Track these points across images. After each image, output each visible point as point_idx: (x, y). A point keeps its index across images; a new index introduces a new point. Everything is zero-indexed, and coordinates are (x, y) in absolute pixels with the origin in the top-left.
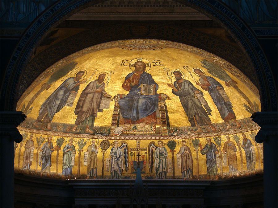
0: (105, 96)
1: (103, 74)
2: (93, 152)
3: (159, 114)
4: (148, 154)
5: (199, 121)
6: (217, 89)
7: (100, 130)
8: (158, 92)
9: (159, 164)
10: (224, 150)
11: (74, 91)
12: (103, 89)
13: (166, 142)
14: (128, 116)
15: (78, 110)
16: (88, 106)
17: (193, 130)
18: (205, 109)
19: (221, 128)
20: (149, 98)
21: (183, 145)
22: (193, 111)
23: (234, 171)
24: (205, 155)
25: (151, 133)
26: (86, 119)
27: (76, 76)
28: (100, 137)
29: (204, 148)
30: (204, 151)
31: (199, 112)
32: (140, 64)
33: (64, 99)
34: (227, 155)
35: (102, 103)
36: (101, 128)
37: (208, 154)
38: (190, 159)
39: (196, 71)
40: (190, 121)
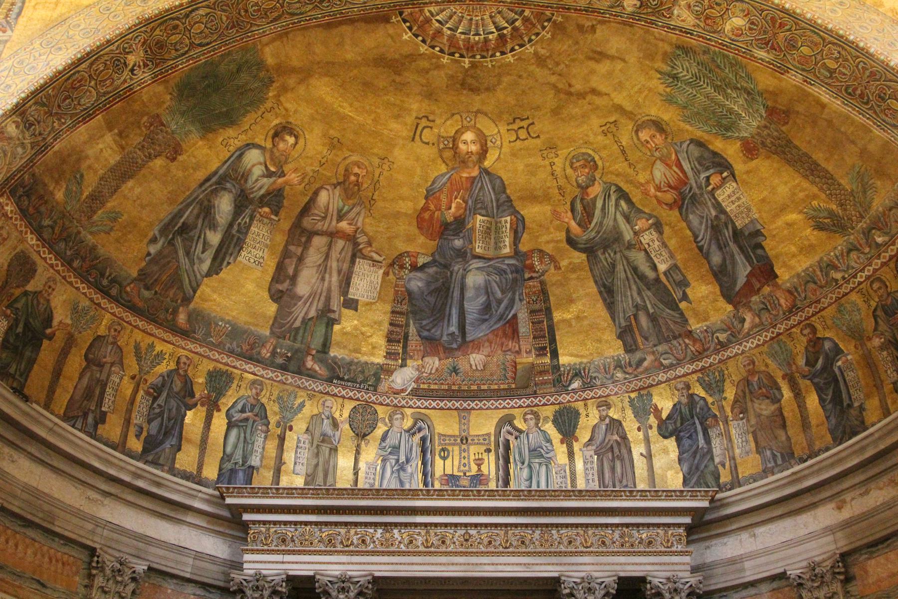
0: (364, 251)
1: (358, 164)
2: (325, 438)
3: (524, 327)
4: (493, 453)
5: (649, 329)
6: (710, 188)
7: (349, 370)
8: (523, 248)
9: (527, 483)
10: (735, 410)
11: (266, 209)
12: (359, 224)
13: (548, 412)
14: (436, 332)
15: (280, 287)
16: (314, 281)
17: (630, 365)
18: (667, 284)
19: (723, 337)
20: (495, 268)
21: (602, 419)
22: (630, 299)
23: (779, 462)
24: (671, 443)
25: (502, 387)
26: (305, 322)
27: (269, 145)
29: (669, 417)
32: (469, 136)
33: (234, 232)
34: (748, 421)
35: (355, 280)
36: (351, 363)
37: (682, 434)
38: (626, 456)
39: (644, 135)
40: (620, 336)
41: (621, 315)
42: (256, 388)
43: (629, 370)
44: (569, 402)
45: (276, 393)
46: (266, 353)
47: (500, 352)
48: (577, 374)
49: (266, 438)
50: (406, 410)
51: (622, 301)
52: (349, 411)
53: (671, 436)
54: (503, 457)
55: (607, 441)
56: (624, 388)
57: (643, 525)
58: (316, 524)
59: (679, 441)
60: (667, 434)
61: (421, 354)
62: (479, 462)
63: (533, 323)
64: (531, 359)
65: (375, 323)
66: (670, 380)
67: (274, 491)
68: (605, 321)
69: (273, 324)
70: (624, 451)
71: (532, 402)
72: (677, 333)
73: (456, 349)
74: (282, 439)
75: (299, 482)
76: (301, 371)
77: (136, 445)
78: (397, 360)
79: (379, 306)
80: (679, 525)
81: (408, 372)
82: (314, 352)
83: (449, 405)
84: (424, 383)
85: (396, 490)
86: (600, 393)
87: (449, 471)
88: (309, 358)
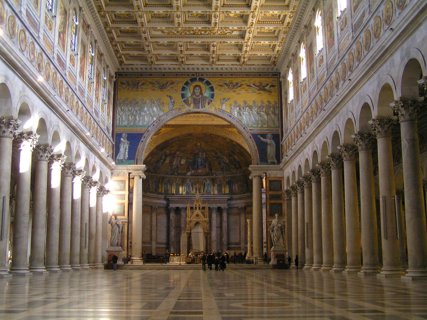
2: (178, 183)
3: (207, 166)
8: (207, 156)
24: (228, 185)
32: (199, 144)
74: (172, 185)
77: (154, 191)
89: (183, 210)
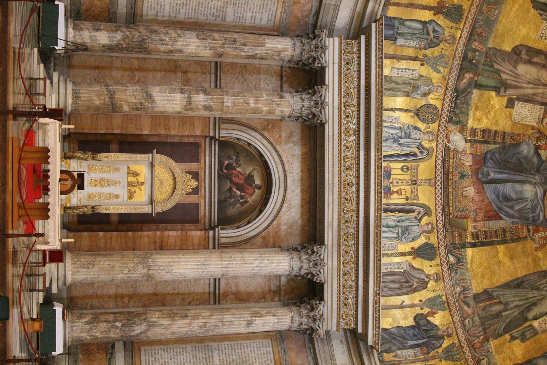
2: (416, 88)
3: (493, 225)
4: (406, 202)
5: (490, 311)
7: (463, 103)
9: (385, 224)
13: (433, 240)
14: (490, 163)
17: (465, 297)
21: (428, 276)
24: (411, 322)
25: (451, 209)
26: (498, 72)
28: (447, 102)
29: (428, 322)
30: (421, 322)
31: (513, 313)
36: (468, 104)
37: (417, 330)
38: (402, 291)
40: (485, 291)
41: (501, 293)
42: (450, 40)
43: (462, 296)
44: (440, 254)
45: (447, 53)
46: (475, 45)
47: (475, 207)
48: (460, 260)
49: (416, 48)
50: (435, 143)
51: (511, 294)
52: (434, 104)
53: (416, 322)
54: (403, 209)
55: (413, 278)
56: (449, 292)
57: (357, 301)
58: (359, 85)
59: (412, 327)
60: (417, 320)
61: (475, 153)
62: (399, 192)
63: (496, 231)
64: (470, 229)
65: (497, 121)
66: (454, 325)
67: (380, 56)
68: (497, 282)
69: (496, 49)
70: (405, 290)
71: (440, 229)
72: (487, 331)
73: (477, 177)
74: (415, 59)
75: (386, 72)
76: (462, 70)
78: (470, 135)
79: (509, 123)
80: (356, 324)
81: (461, 144)
82: (476, 78)
83: (439, 172)
84: (454, 155)
85: (382, 137)
86: (446, 275)
87: (393, 172)
88: (472, 75)
89: (307, 104)
